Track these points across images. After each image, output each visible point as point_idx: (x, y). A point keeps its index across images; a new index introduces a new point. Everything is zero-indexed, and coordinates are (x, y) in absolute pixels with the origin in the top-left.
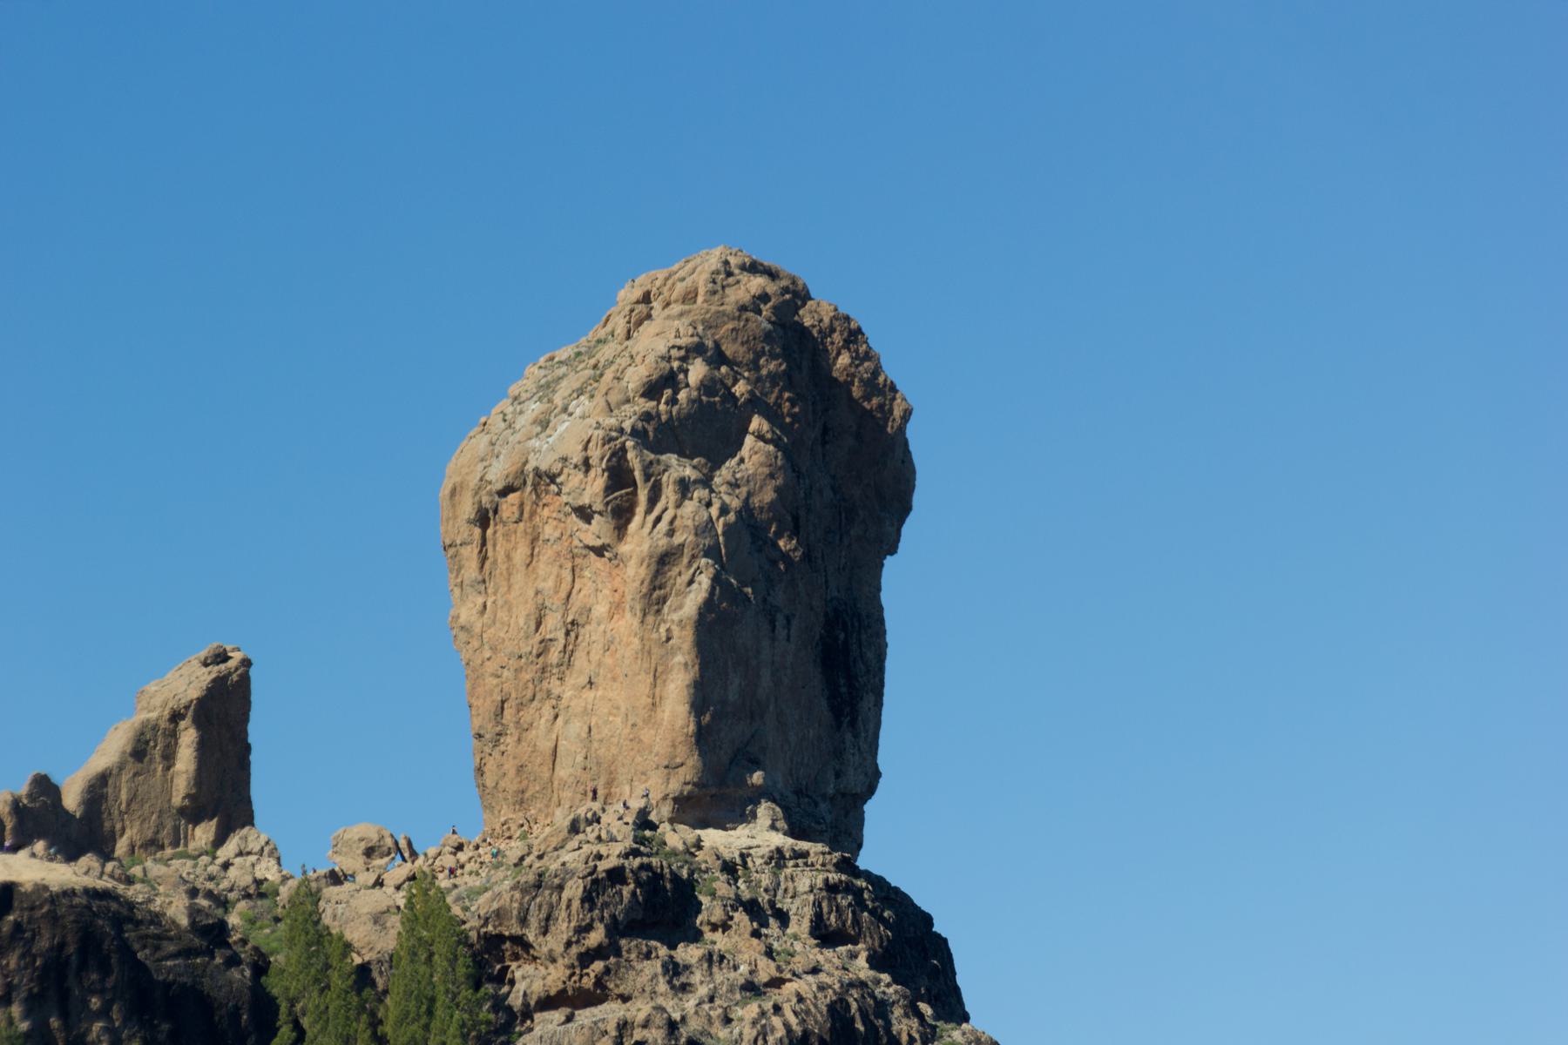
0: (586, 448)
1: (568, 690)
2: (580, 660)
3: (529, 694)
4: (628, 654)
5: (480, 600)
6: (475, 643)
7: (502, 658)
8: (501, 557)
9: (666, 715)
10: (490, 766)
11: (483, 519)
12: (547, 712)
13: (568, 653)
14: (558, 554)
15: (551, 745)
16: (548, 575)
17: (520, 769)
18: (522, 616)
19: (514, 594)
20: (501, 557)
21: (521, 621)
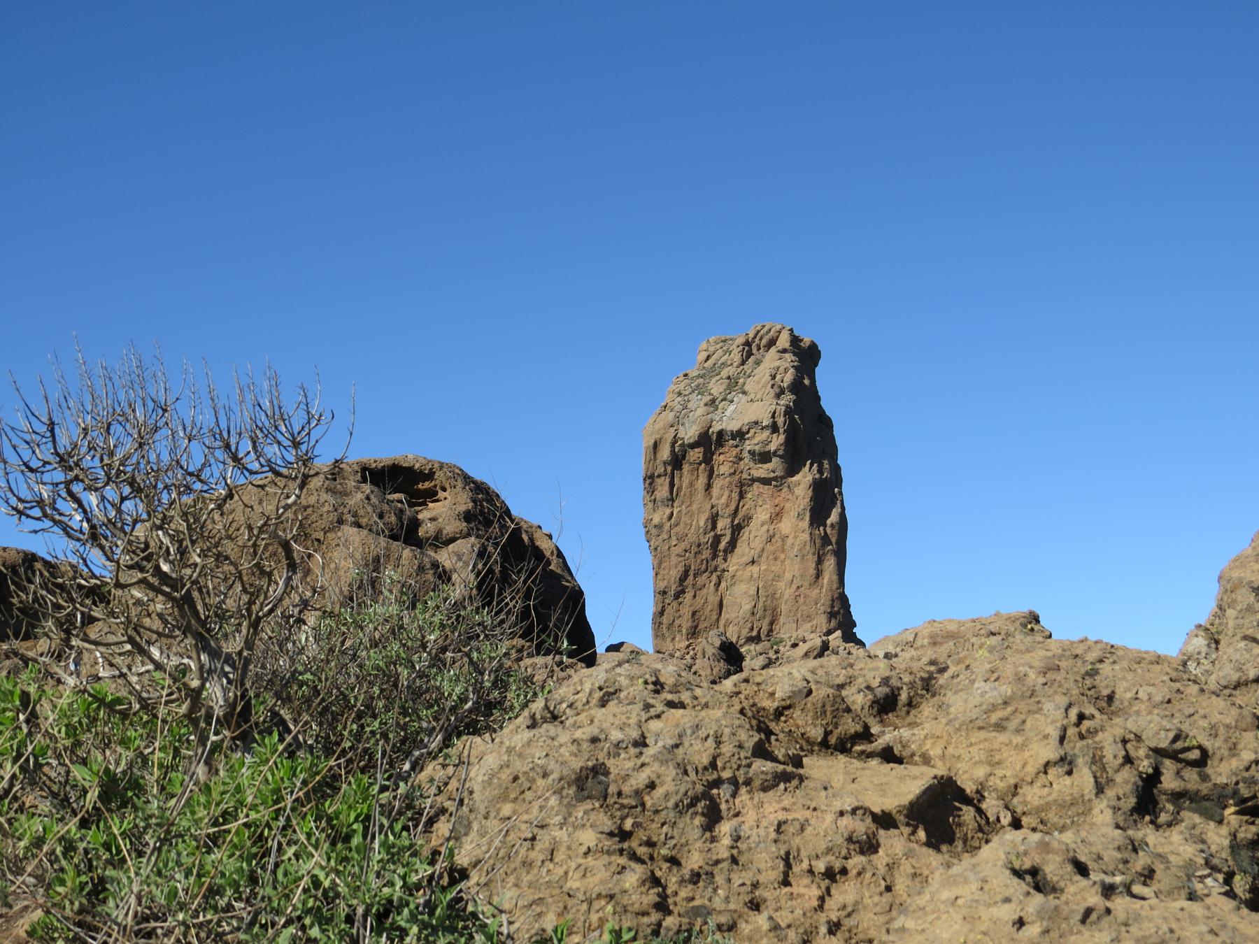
0: (773, 416)
1: (734, 563)
2: (742, 547)
3: (703, 567)
4: (798, 542)
5: (668, 511)
6: (665, 536)
7: (683, 546)
8: (685, 483)
9: (826, 581)
10: (669, 610)
11: (677, 462)
12: (714, 578)
13: (733, 545)
14: (731, 483)
15: (718, 599)
16: (722, 495)
17: (694, 613)
18: (702, 520)
19: (694, 507)
20: (685, 483)
21: (702, 524)
